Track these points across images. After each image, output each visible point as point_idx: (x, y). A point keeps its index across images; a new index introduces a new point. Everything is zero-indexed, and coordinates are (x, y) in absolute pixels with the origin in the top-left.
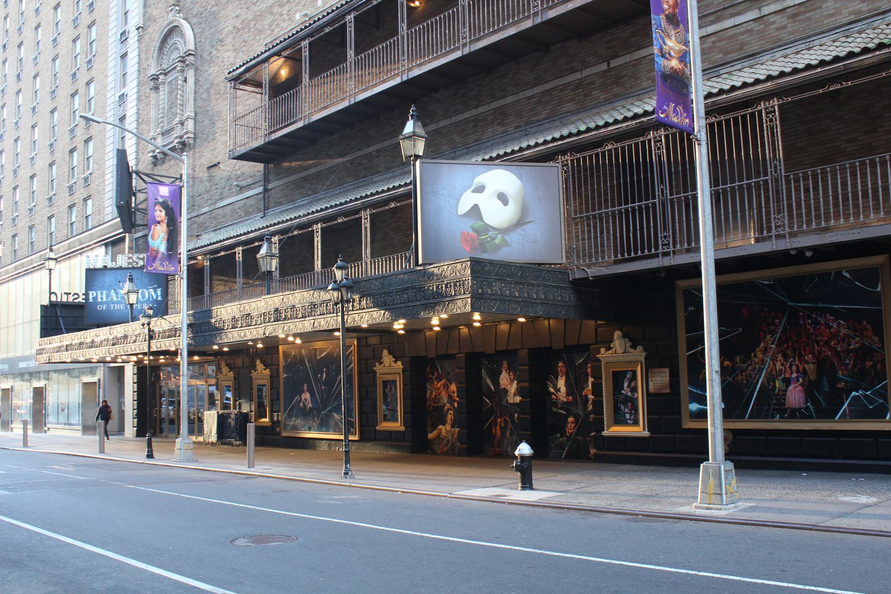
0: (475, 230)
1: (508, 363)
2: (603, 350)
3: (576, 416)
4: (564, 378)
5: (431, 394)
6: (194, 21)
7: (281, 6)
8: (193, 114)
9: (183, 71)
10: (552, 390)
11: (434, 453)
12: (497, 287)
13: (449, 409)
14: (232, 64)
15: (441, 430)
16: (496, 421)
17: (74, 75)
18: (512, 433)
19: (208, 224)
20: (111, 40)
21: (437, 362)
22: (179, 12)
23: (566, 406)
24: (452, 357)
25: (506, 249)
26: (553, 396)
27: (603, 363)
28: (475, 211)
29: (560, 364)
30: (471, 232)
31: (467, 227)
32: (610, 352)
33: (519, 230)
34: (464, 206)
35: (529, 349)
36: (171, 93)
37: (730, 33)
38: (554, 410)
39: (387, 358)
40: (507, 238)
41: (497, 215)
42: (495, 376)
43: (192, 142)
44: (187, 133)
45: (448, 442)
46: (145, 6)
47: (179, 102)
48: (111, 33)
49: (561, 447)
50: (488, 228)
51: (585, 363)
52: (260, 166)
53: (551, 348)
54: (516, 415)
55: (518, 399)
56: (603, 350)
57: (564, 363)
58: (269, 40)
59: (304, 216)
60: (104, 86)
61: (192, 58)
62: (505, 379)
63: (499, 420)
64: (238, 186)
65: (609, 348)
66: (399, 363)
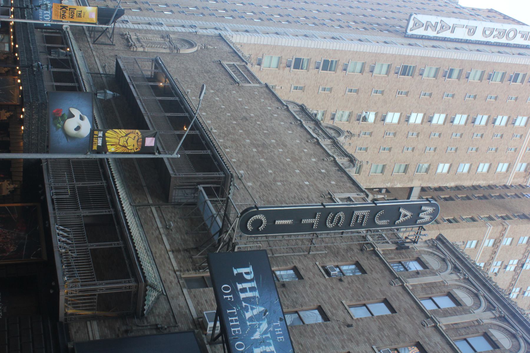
0: (63, 115)
6: (195, 54)
7: (195, 85)
8: (146, 51)
9: (170, 48)
12: (35, 116)
14: (170, 67)
17: (177, 6)
19: (87, 54)
20: (193, 22)
22: (201, 48)
25: (55, 128)
28: (72, 116)
30: (62, 113)
31: (65, 112)
33: (63, 135)
34: (74, 111)
36: (160, 44)
37: (153, 221)
39: (8, 114)
40: (60, 129)
41: (71, 125)
43: (132, 50)
44: (136, 47)
46: (208, 36)
47: (153, 46)
48: (196, 22)
50: (64, 121)
52: (114, 74)
58: (179, 80)
59: (82, 79)
60: (169, 18)
61: (176, 51)
64: (105, 66)
66: (6, 118)
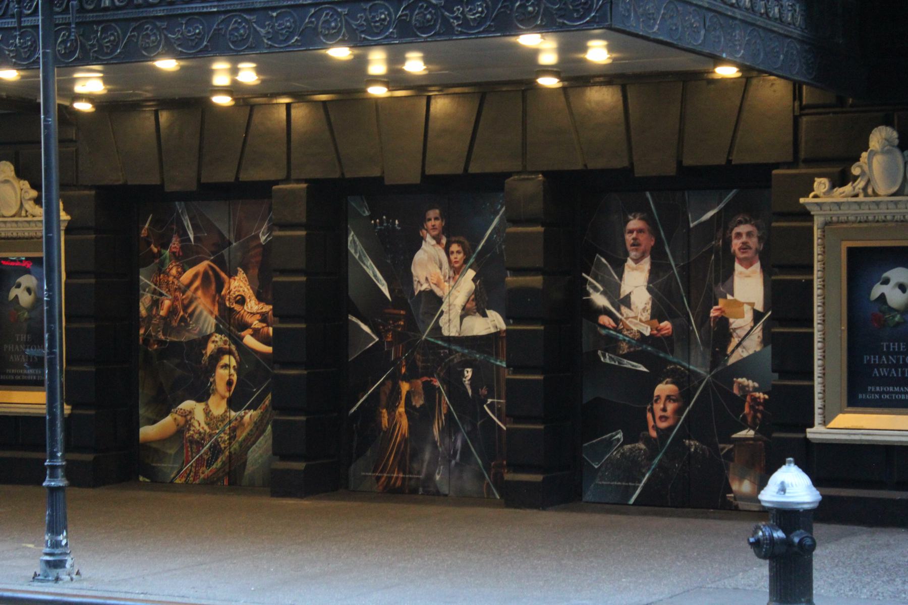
1: (442, 216)
2: (821, 185)
3: (686, 383)
4: (646, 264)
5: (156, 304)
10: (600, 300)
11: (158, 482)
13: (220, 352)
15: (188, 415)
16: (396, 391)
18: (450, 427)
21: (179, 206)
23: (649, 349)
24: (261, 191)
26: (604, 320)
27: (818, 222)
29: (634, 223)
32: (848, 188)
35: (553, 177)
38: (607, 359)
42: (398, 256)
45: (216, 450)
49: (629, 469)
51: (723, 223)
53: (630, 169)
54: (468, 373)
55: (491, 323)
56: (821, 185)
57: (649, 219)
62: (430, 264)
63: (405, 387)
65: (842, 179)
